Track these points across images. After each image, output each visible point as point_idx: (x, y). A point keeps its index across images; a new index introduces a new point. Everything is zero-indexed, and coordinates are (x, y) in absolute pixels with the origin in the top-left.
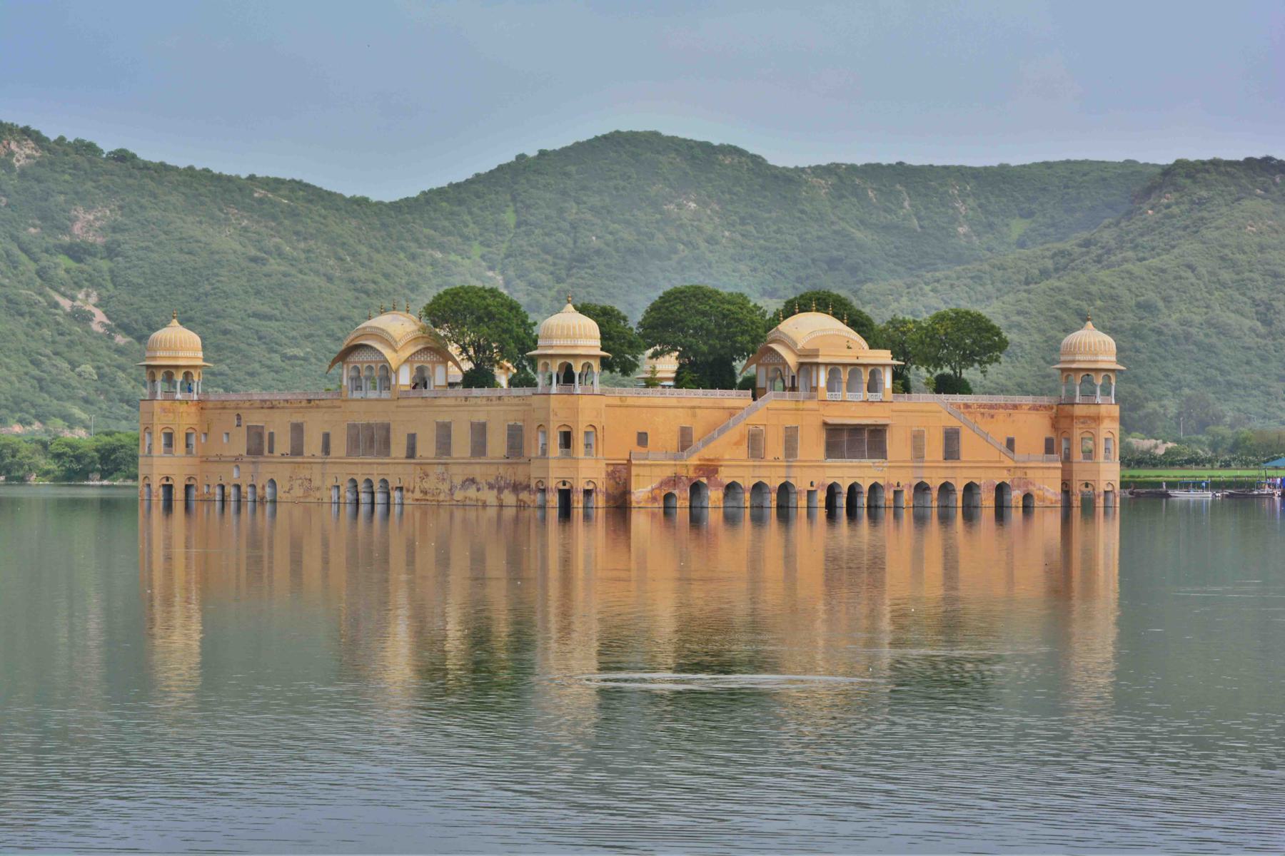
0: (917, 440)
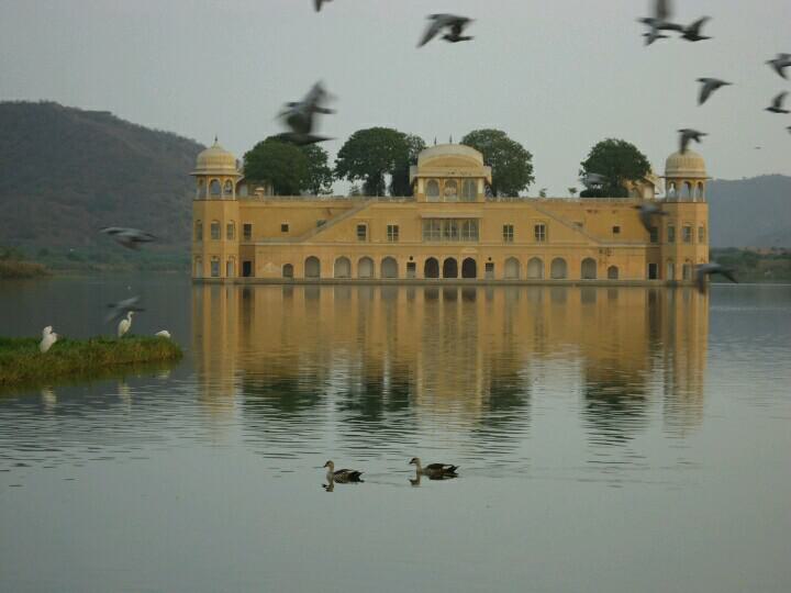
0: (508, 231)
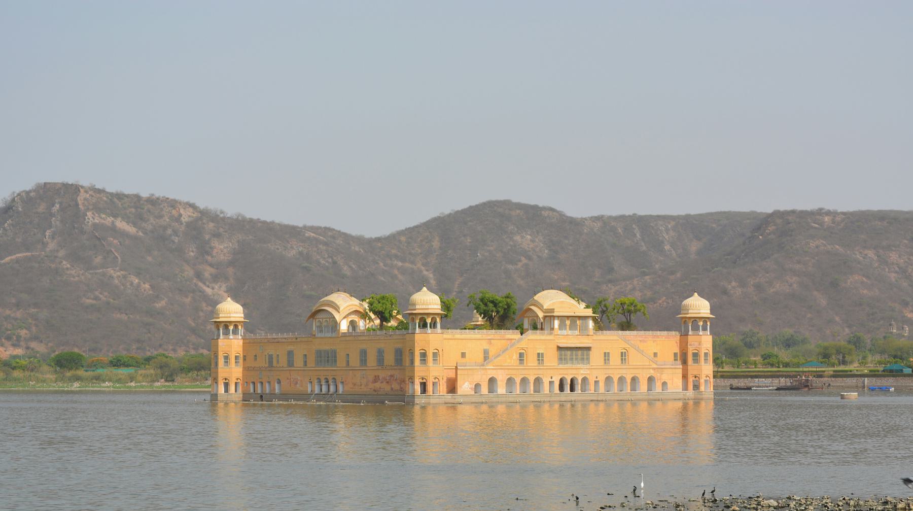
0: (606, 355)
